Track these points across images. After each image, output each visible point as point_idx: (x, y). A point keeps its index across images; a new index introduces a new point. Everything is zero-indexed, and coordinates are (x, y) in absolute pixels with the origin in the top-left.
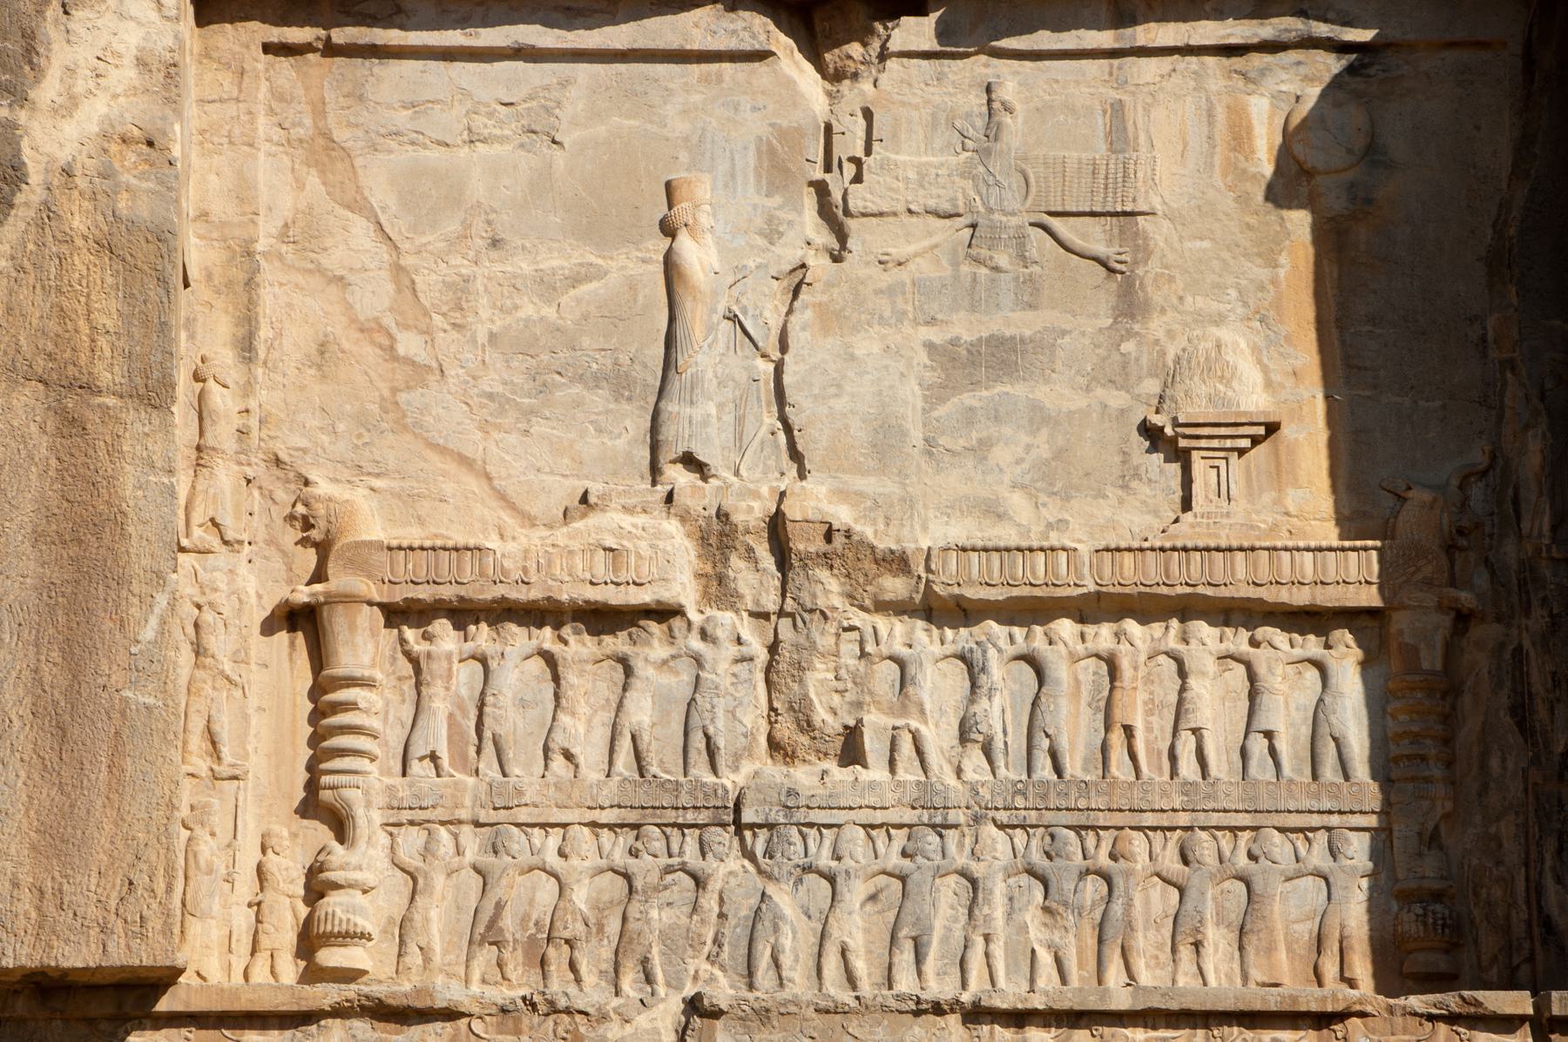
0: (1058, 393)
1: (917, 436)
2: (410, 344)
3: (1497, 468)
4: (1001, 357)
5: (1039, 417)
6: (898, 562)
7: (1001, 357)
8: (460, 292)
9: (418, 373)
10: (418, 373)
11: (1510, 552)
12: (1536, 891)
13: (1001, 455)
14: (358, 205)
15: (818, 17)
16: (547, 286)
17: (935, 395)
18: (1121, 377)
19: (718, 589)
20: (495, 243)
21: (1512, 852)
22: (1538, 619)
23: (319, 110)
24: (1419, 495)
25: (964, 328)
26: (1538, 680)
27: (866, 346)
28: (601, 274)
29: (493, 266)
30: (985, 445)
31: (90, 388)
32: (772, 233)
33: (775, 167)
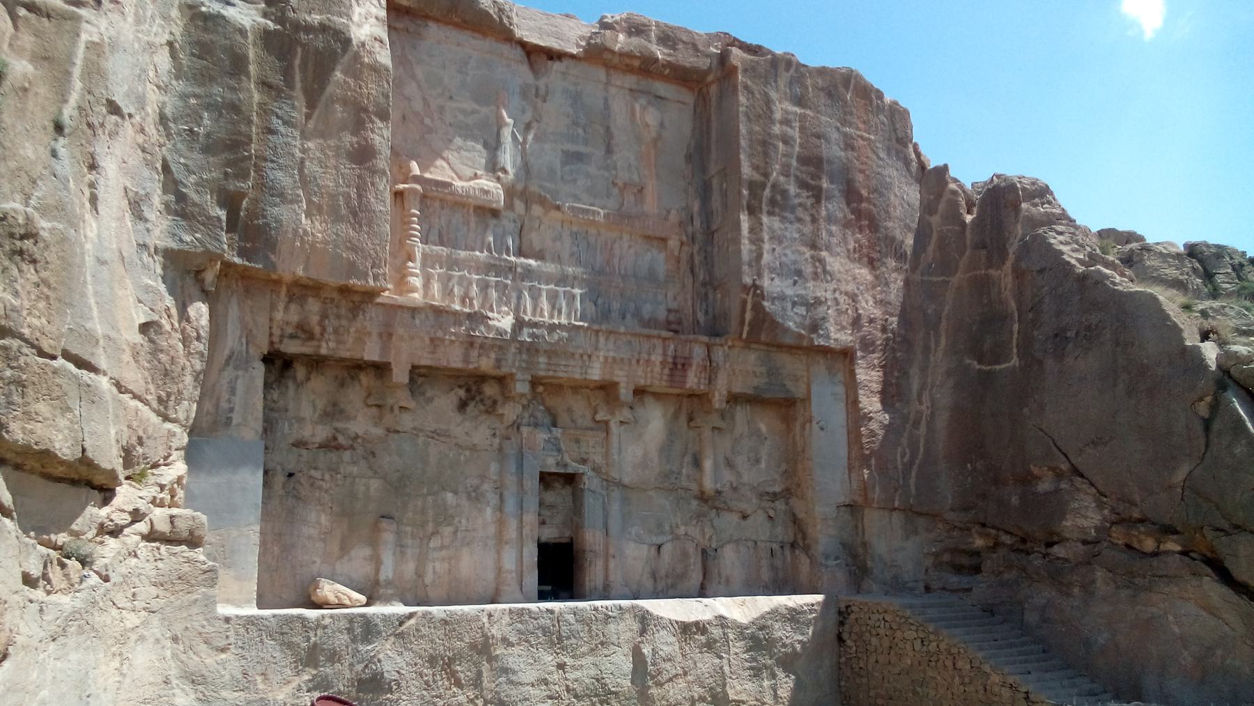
0: (592, 170)
1: (559, 173)
2: (427, 121)
3: (687, 208)
4: (578, 157)
5: (588, 175)
6: (558, 208)
7: (578, 157)
8: (442, 109)
9: (430, 131)
10: (430, 131)
11: (690, 229)
12: (694, 312)
13: (580, 183)
14: (413, 77)
15: (533, 57)
16: (464, 112)
17: (564, 164)
18: (607, 168)
19: (509, 205)
20: (451, 98)
21: (690, 303)
22: (696, 247)
23: (403, 49)
24: (673, 212)
25: (572, 148)
26: (697, 262)
27: (547, 146)
28: (479, 112)
29: (450, 104)
30: (575, 181)
31: (366, 110)
32: (524, 112)
33: (524, 94)
